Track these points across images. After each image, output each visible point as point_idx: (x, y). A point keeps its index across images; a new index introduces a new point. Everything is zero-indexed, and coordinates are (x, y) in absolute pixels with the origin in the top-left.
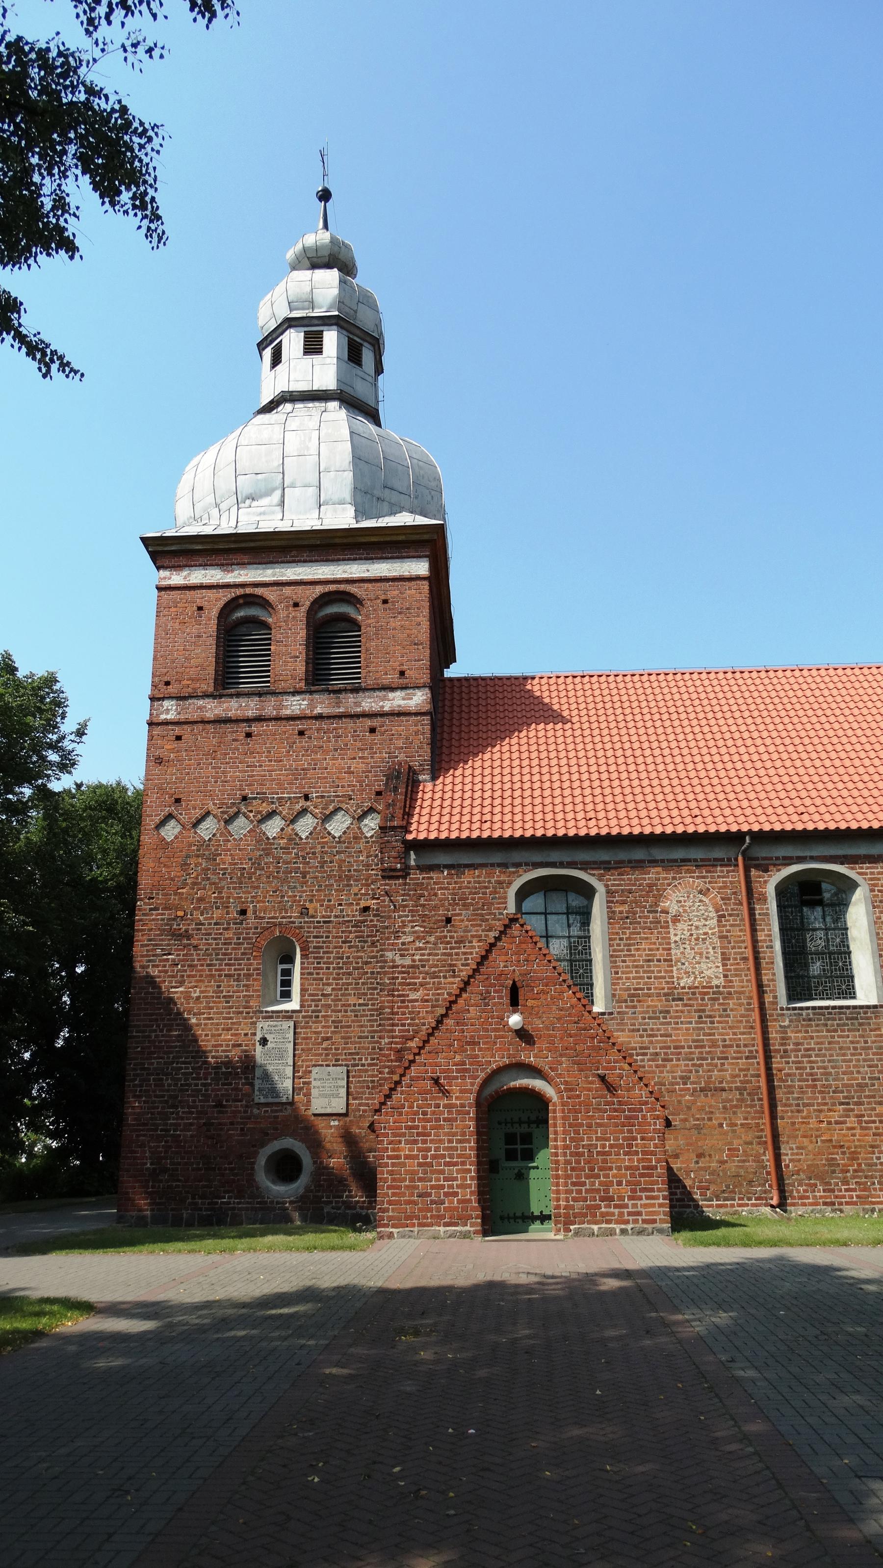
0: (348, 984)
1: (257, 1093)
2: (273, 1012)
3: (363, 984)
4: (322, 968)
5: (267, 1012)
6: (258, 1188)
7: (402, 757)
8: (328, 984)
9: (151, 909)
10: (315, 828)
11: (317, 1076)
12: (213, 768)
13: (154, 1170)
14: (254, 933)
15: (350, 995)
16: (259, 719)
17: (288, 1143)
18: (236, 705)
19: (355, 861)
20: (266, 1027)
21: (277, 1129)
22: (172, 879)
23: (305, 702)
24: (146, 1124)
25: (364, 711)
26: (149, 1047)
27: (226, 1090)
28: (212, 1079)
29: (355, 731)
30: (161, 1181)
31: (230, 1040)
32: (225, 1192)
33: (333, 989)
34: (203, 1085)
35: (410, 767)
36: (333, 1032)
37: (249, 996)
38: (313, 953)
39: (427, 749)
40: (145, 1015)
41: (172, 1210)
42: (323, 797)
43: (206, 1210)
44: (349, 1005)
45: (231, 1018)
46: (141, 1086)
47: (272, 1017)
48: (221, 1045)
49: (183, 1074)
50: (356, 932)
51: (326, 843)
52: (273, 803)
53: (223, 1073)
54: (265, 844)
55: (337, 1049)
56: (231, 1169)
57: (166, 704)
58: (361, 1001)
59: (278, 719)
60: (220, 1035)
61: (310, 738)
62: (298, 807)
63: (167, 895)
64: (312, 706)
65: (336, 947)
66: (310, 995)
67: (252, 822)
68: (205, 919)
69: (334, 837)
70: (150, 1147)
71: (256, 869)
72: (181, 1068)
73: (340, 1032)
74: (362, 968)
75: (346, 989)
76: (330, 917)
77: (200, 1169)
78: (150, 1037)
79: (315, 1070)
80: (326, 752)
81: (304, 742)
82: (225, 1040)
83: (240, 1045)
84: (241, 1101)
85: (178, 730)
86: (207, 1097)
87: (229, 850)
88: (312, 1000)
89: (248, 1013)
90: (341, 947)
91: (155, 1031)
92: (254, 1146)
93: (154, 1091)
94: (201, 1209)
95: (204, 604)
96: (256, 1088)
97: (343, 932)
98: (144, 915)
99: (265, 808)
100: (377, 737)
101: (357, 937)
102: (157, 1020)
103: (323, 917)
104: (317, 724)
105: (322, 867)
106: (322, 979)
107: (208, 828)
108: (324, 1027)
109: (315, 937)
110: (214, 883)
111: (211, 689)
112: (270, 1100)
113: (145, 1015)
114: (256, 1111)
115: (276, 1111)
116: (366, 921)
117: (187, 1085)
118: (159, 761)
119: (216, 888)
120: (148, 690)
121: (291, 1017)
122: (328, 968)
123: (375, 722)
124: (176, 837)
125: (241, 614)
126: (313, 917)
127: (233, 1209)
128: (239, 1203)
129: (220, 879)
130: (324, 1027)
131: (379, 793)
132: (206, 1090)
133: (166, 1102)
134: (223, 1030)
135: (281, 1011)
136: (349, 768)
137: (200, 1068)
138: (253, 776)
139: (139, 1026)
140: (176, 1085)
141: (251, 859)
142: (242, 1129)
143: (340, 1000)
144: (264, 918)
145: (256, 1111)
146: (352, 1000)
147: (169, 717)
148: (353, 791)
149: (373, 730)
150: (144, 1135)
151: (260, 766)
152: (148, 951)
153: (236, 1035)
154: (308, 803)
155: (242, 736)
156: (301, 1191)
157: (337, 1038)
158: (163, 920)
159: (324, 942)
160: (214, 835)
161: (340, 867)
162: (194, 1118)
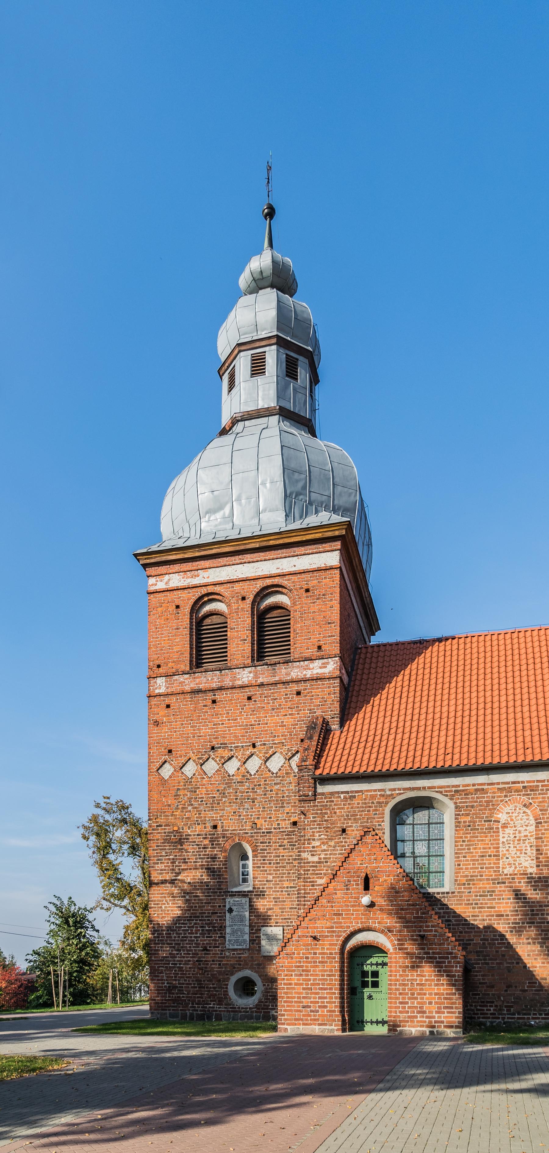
1: (227, 942)
2: (236, 892)
3: (293, 873)
4: (266, 864)
5: (232, 892)
6: (230, 999)
7: (319, 713)
8: (270, 874)
9: (157, 826)
10: (260, 767)
12: (192, 727)
13: (169, 987)
14: (222, 841)
15: (284, 881)
16: (221, 689)
17: (247, 973)
18: (205, 679)
19: (287, 790)
20: (232, 902)
21: (240, 965)
22: (169, 806)
23: (252, 675)
24: (162, 961)
25: (292, 679)
26: (162, 914)
27: (209, 940)
28: (200, 934)
29: (286, 695)
30: (173, 994)
31: (210, 910)
32: (211, 1001)
33: (273, 877)
34: (195, 937)
35: (324, 719)
36: (274, 905)
37: (221, 882)
38: (260, 853)
39: (337, 705)
40: (158, 894)
41: (181, 1010)
42: (265, 744)
43: (200, 1011)
44: (284, 887)
45: (210, 896)
46: (158, 937)
47: (235, 895)
48: (205, 913)
49: (183, 930)
50: (288, 839)
51: (268, 777)
52: (231, 750)
53: (207, 930)
54: (228, 780)
55: (276, 916)
56: (214, 988)
57: (159, 681)
59: (233, 688)
61: (255, 701)
62: (248, 753)
63: (167, 816)
64: (256, 677)
66: (259, 881)
67: (218, 764)
68: (191, 832)
69: (273, 773)
70: (166, 974)
71: (222, 797)
72: (181, 927)
73: (278, 905)
74: (292, 863)
76: (271, 829)
77: (196, 987)
78: (161, 907)
80: (266, 712)
81: (251, 704)
82: (207, 910)
83: (216, 913)
84: (218, 947)
85: (167, 701)
86: (198, 944)
87: (204, 785)
89: (220, 892)
90: (278, 849)
91: (164, 904)
92: (227, 975)
93: (166, 941)
94: (197, 1010)
95: (180, 603)
96: (227, 940)
97: (279, 839)
98: (153, 830)
99: (226, 754)
100: (301, 698)
101: (288, 842)
102: (165, 897)
103: (266, 829)
104: (259, 691)
105: (265, 794)
107: (190, 769)
109: (261, 843)
110: (196, 808)
111: (188, 669)
112: (236, 947)
113: (158, 894)
114: (227, 954)
115: (240, 954)
116: (294, 831)
117: (185, 937)
118: (157, 723)
119: (197, 811)
120: (146, 673)
121: (247, 895)
122: (270, 863)
123: (301, 687)
124: (170, 777)
125: (207, 608)
126: (260, 829)
127: (216, 1011)
128: (220, 1008)
129: (199, 805)
131: (302, 740)
132: (197, 941)
133: (174, 947)
135: (241, 892)
136: (282, 722)
137: (193, 927)
138: (218, 731)
139: (155, 901)
140: (179, 937)
141: (218, 791)
142: (220, 964)
143: (278, 884)
144: (228, 830)
145: (227, 954)
146: (286, 884)
147: (161, 691)
148: (285, 739)
149: (298, 693)
150: (163, 967)
151: (223, 724)
152: (157, 853)
153: (213, 906)
154: (255, 750)
155: (209, 702)
156: (256, 1002)
158: (165, 833)
159: (267, 846)
160: (194, 775)
161: (277, 794)
162: (191, 957)
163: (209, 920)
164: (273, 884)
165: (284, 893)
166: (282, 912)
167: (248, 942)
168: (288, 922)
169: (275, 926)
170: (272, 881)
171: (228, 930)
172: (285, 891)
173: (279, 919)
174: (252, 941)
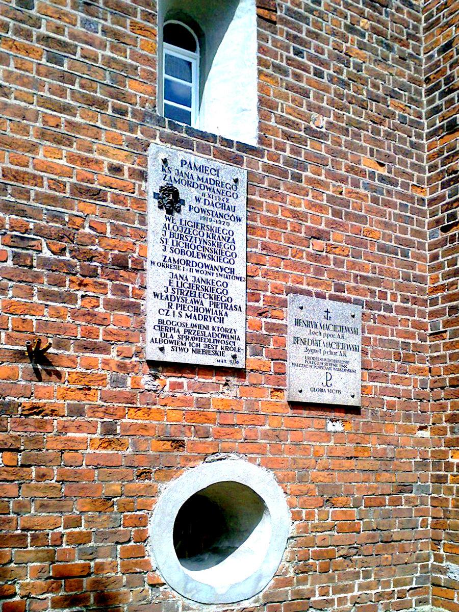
0: (360, 127)
11: (302, 315)
15: (362, 149)
36: (329, 223)
44: (362, 173)
58: (383, 171)
60: (33, 148)
65: (334, 34)
66: (282, 121)
75: (357, 136)
79: (295, 303)
82: (49, 169)
88: (288, 137)
96: (151, 320)
106: (306, 94)
108: (311, 205)
121: (237, 161)
122: (319, 74)
130: (311, 205)
134: (42, 135)
153: (86, 162)
157: (337, 237)
163: (56, 217)
164: (329, 150)
165: (362, 191)
166: (357, 255)
167: (241, 344)
168: (373, 292)
169: (332, 298)
170: (325, 136)
171: (157, 279)
172: (367, 187)
173: (346, 276)
174: (256, 342)
